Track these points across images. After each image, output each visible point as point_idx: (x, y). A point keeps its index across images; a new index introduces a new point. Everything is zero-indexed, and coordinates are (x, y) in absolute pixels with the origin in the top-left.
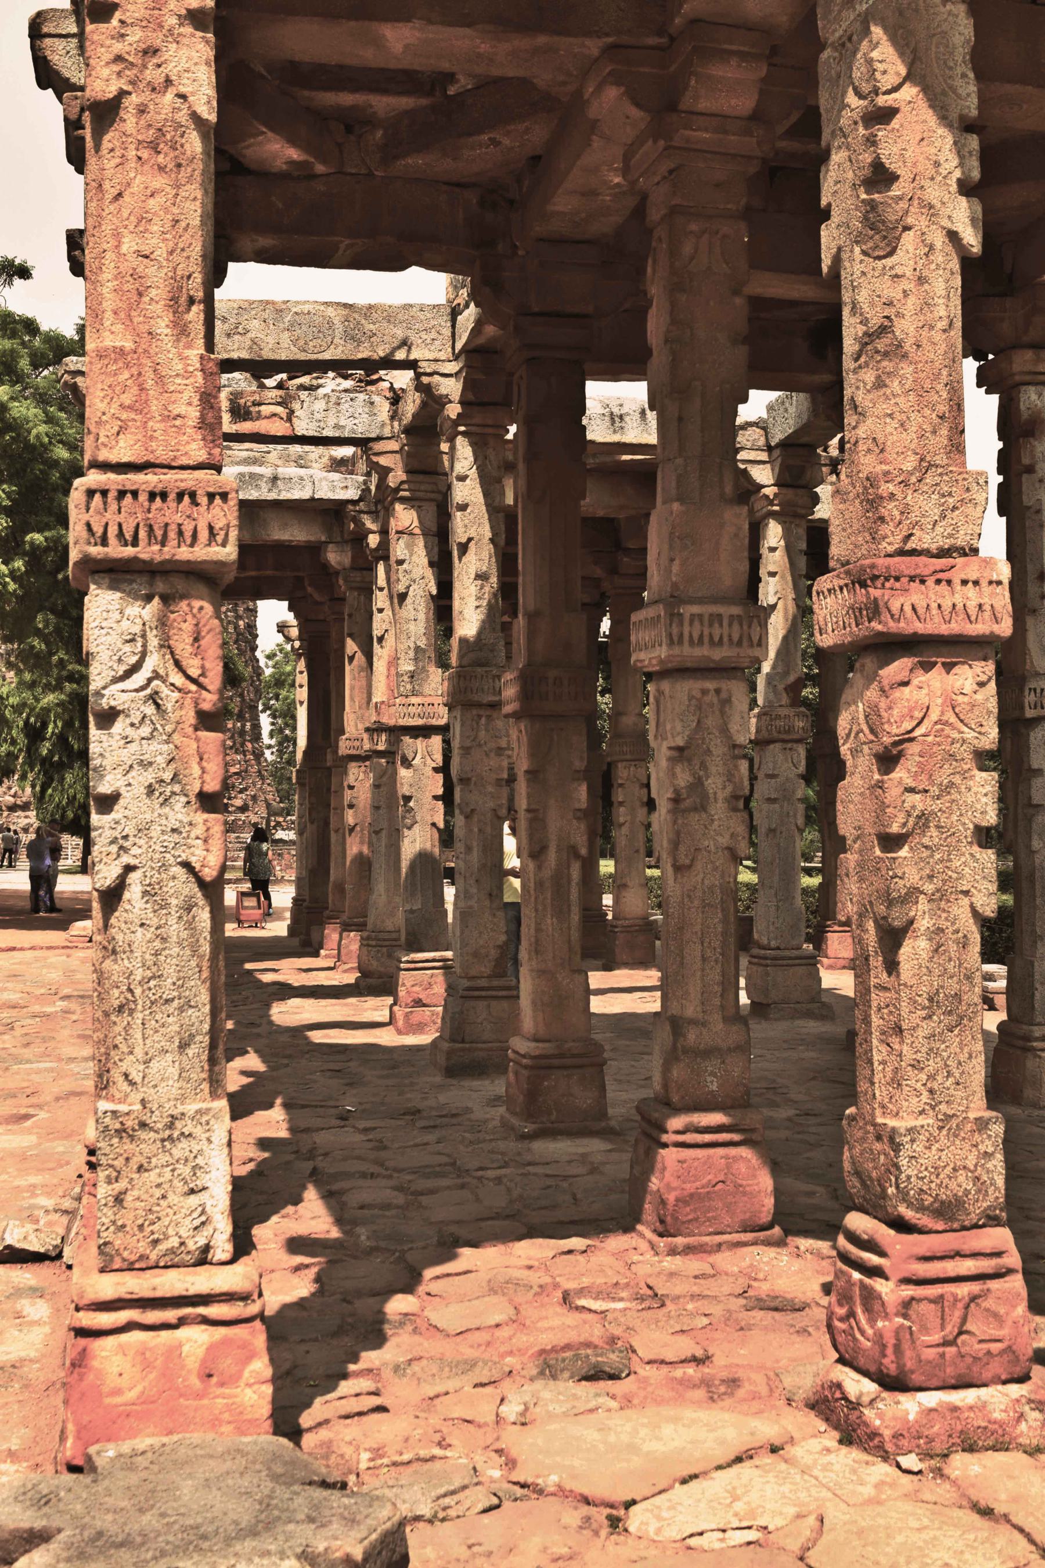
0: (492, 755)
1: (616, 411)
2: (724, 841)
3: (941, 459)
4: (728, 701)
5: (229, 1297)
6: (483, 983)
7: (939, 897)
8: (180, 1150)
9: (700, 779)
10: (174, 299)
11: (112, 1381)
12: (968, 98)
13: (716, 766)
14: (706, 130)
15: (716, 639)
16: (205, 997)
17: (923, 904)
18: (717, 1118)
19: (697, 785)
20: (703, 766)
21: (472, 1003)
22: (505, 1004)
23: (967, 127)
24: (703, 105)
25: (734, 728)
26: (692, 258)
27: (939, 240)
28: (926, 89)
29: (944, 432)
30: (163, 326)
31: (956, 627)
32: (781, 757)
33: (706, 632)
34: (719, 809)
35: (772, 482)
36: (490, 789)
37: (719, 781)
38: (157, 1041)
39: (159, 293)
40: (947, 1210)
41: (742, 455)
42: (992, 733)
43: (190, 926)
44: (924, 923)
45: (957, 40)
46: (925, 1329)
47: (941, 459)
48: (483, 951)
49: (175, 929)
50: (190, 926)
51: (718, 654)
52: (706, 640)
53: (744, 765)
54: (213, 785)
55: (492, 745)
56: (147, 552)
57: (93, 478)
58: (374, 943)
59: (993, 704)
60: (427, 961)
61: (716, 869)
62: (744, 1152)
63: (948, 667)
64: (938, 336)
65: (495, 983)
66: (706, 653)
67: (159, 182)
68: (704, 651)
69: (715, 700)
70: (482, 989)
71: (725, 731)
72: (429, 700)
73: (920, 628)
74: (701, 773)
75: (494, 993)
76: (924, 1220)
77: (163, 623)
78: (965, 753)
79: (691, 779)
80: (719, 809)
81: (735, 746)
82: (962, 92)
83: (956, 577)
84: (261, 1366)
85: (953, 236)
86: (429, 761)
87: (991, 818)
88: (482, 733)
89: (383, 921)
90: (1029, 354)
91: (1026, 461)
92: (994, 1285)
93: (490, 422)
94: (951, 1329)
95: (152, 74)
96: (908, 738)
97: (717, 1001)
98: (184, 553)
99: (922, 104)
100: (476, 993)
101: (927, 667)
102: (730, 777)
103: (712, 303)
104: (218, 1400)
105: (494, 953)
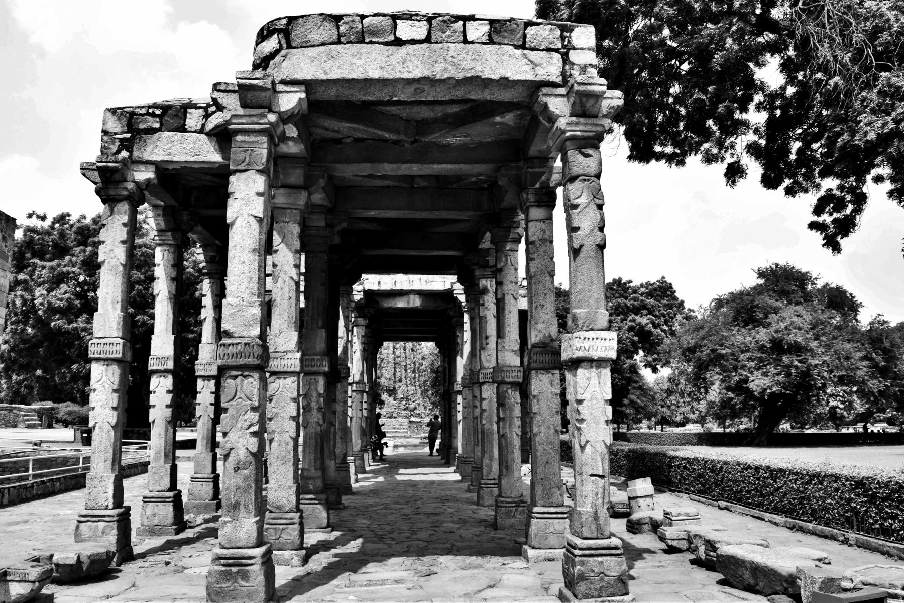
2: (316, 420)
3: (285, 330)
5: (109, 516)
7: (281, 432)
8: (103, 484)
10: (113, 302)
11: (83, 533)
12: (297, 244)
13: (314, 399)
16: (111, 451)
17: (276, 434)
18: (311, 496)
19: (309, 404)
23: (298, 252)
27: (287, 279)
28: (287, 245)
29: (286, 323)
30: (110, 308)
31: (285, 369)
32: (467, 393)
34: (315, 412)
38: (100, 460)
39: (109, 301)
40: (278, 507)
42: (296, 394)
43: (109, 435)
44: (276, 439)
45: (295, 232)
46: (271, 535)
47: (285, 330)
49: (105, 436)
50: (109, 435)
51: (313, 369)
53: (322, 399)
54: (115, 405)
56: (102, 356)
57: (95, 341)
59: (296, 387)
62: (319, 506)
63: (285, 378)
64: (286, 302)
67: (112, 278)
68: (310, 368)
71: (317, 390)
73: (276, 370)
76: (273, 510)
77: (107, 370)
78: (288, 399)
80: (315, 412)
83: (286, 357)
84: (115, 531)
85: (292, 278)
87: (295, 414)
91: (481, 302)
92: (290, 526)
94: (277, 536)
95: (112, 255)
96: (273, 395)
98: (110, 356)
99: (285, 248)
101: (280, 378)
102: (318, 402)
104: (105, 538)
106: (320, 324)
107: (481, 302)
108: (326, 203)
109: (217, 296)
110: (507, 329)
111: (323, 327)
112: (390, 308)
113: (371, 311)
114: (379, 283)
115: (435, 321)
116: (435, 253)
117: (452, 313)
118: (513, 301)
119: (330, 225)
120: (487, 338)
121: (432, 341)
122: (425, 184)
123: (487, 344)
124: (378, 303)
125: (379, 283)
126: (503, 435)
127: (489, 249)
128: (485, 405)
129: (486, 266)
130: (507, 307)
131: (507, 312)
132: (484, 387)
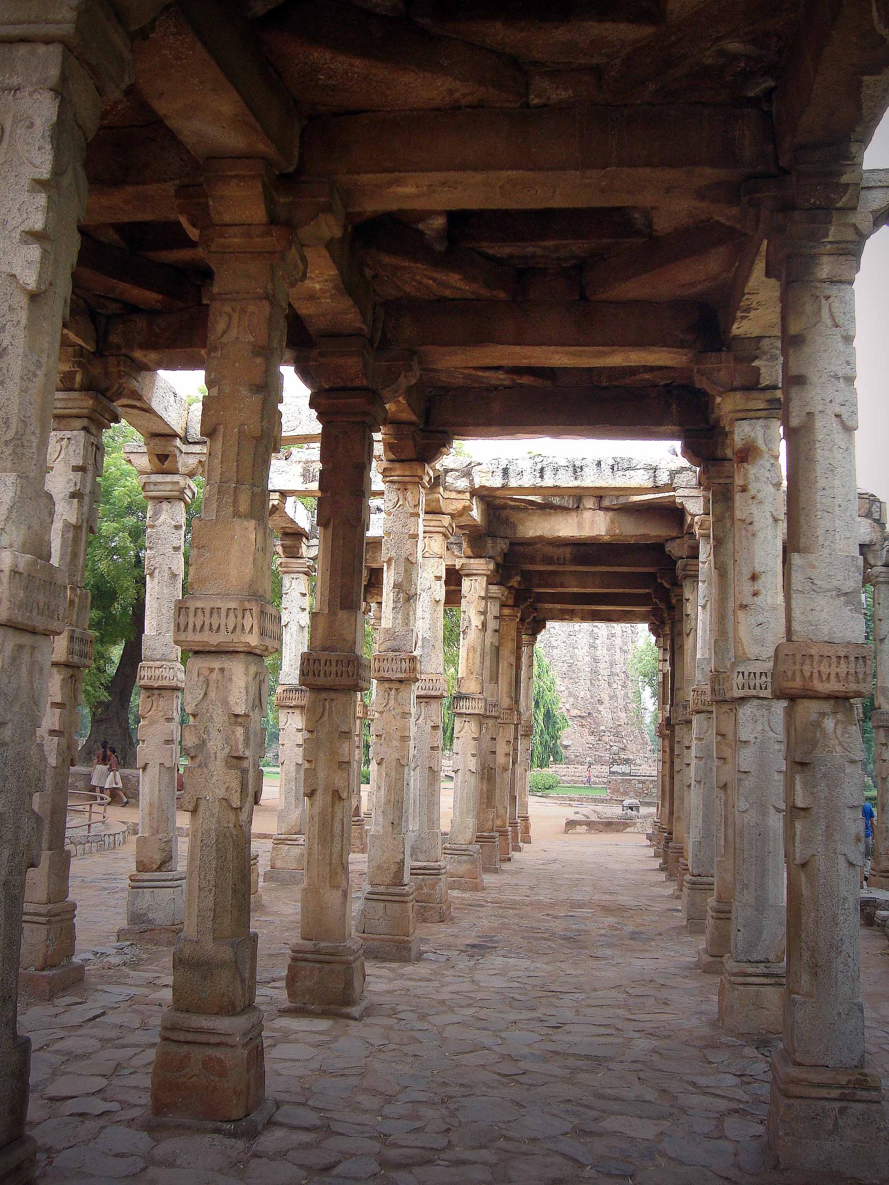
0: (398, 718)
1: (578, 464)
2: (221, 793)
4: (230, 679)
6: (382, 889)
9: (204, 741)
14: (235, 236)
15: (215, 627)
20: (206, 730)
21: (374, 904)
22: (397, 906)
24: (227, 218)
25: (232, 700)
26: (224, 333)
33: (207, 623)
34: (218, 767)
35: (702, 512)
36: (395, 743)
37: (219, 744)
41: (680, 492)
48: (385, 865)
51: (214, 640)
52: (207, 627)
53: (240, 731)
55: (399, 710)
58: (449, 852)
60: (420, 869)
61: (212, 815)
65: (397, 890)
66: (206, 639)
69: (220, 677)
70: (381, 894)
71: (225, 703)
72: (430, 677)
74: (205, 736)
75: (390, 898)
79: (197, 741)
81: (237, 716)
82: (38, 162)
86: (429, 721)
88: (392, 702)
89: (457, 837)
90: (738, 395)
93: (408, 473)
97: (209, 924)
100: (376, 897)
102: (227, 740)
103: (237, 365)
105: (394, 868)
106: (244, 506)
107: (739, 481)
108: (261, 147)
109: (76, 469)
110: (822, 523)
111: (250, 515)
112: (541, 539)
113: (502, 545)
114: (505, 472)
115: (640, 571)
116: (618, 359)
117: (675, 549)
118: (839, 436)
119: (273, 221)
120: (754, 578)
121: (643, 619)
122: (560, 94)
123: (755, 594)
124: (514, 526)
125: (505, 472)
126: (804, 865)
127: (760, 338)
128: (746, 759)
129: (752, 386)
130: (820, 454)
131: (820, 468)
132: (746, 712)
